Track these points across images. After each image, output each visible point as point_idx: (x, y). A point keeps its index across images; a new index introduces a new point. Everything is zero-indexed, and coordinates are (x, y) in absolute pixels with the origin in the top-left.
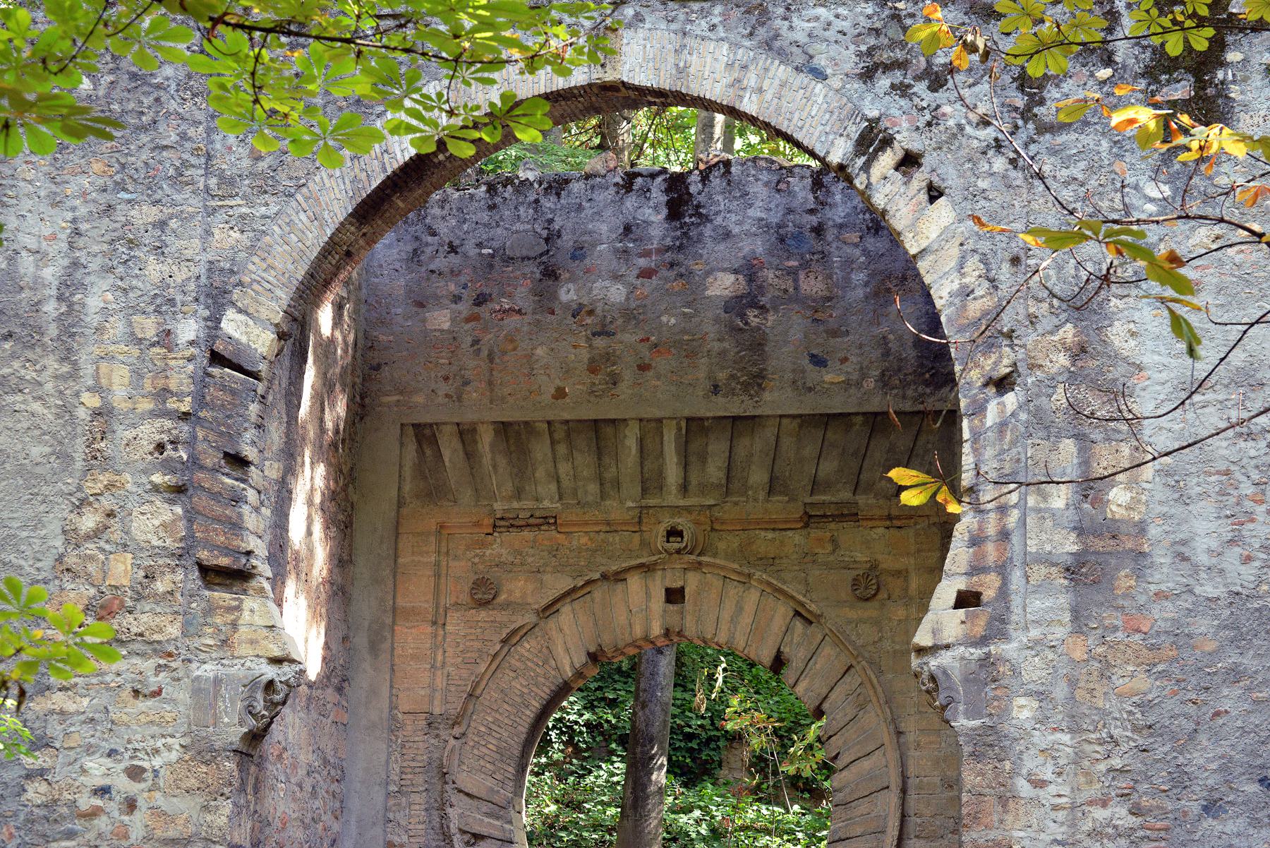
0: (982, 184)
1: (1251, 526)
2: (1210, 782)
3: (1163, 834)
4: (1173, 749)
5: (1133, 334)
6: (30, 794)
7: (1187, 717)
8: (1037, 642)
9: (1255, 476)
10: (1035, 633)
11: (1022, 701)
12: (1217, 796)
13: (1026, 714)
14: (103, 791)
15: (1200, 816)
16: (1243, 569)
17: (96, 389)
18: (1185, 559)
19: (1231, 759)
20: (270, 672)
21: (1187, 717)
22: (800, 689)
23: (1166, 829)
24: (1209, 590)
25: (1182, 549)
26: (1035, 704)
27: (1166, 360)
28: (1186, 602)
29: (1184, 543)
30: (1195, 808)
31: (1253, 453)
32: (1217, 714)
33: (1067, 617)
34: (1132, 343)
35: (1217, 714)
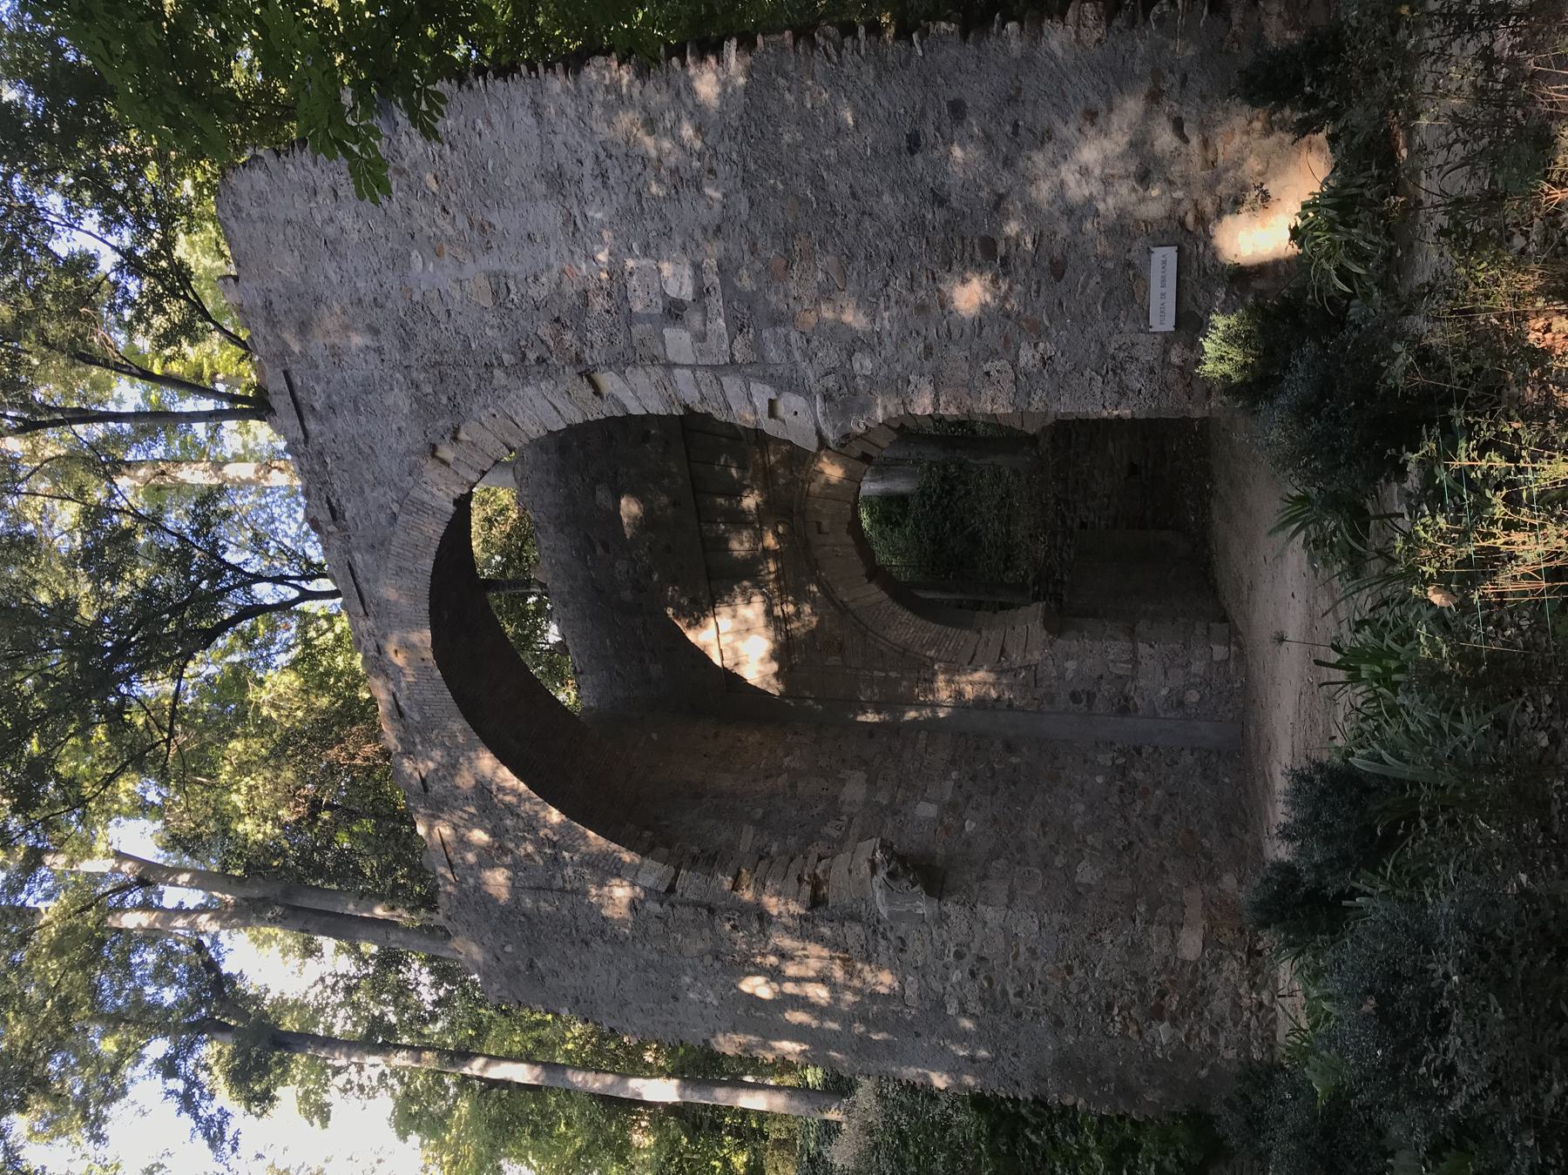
0: (444, 400)
1: (682, 170)
2: (916, 200)
3: (967, 242)
4: (889, 235)
5: (536, 279)
6: (977, 1012)
7: (858, 223)
8: (804, 354)
9: (639, 168)
10: (797, 355)
11: (857, 366)
12: (928, 195)
13: (868, 363)
14: (973, 974)
15: (948, 208)
16: (721, 175)
17: (701, 957)
18: (719, 228)
19: (895, 182)
20: (882, 874)
21: (858, 223)
22: (885, 444)
23: (963, 239)
24: (744, 206)
25: (710, 232)
26: (858, 355)
27: (553, 250)
28: (756, 227)
29: (705, 229)
30: (941, 215)
31: (618, 171)
32: (854, 195)
33: (781, 331)
34: (544, 280)
35: (854, 195)
